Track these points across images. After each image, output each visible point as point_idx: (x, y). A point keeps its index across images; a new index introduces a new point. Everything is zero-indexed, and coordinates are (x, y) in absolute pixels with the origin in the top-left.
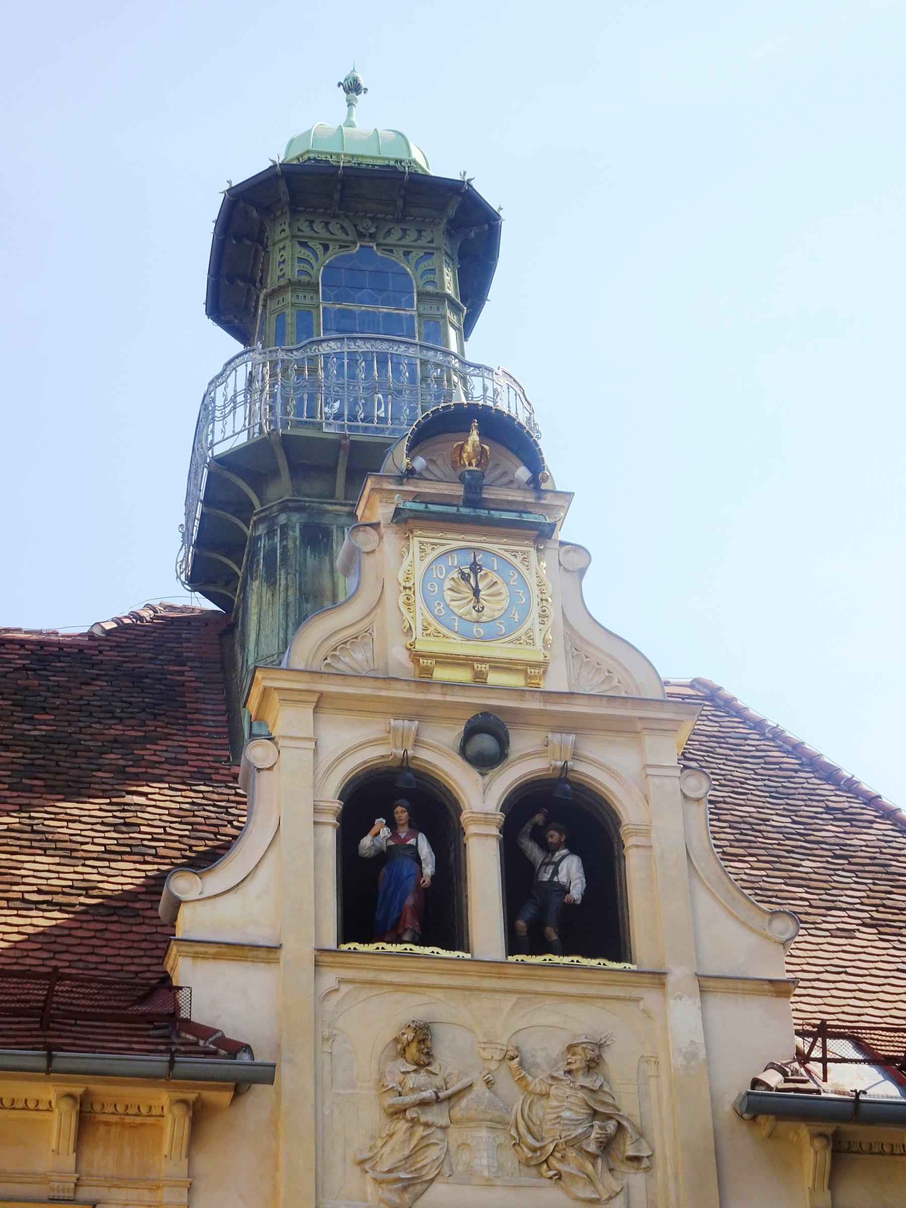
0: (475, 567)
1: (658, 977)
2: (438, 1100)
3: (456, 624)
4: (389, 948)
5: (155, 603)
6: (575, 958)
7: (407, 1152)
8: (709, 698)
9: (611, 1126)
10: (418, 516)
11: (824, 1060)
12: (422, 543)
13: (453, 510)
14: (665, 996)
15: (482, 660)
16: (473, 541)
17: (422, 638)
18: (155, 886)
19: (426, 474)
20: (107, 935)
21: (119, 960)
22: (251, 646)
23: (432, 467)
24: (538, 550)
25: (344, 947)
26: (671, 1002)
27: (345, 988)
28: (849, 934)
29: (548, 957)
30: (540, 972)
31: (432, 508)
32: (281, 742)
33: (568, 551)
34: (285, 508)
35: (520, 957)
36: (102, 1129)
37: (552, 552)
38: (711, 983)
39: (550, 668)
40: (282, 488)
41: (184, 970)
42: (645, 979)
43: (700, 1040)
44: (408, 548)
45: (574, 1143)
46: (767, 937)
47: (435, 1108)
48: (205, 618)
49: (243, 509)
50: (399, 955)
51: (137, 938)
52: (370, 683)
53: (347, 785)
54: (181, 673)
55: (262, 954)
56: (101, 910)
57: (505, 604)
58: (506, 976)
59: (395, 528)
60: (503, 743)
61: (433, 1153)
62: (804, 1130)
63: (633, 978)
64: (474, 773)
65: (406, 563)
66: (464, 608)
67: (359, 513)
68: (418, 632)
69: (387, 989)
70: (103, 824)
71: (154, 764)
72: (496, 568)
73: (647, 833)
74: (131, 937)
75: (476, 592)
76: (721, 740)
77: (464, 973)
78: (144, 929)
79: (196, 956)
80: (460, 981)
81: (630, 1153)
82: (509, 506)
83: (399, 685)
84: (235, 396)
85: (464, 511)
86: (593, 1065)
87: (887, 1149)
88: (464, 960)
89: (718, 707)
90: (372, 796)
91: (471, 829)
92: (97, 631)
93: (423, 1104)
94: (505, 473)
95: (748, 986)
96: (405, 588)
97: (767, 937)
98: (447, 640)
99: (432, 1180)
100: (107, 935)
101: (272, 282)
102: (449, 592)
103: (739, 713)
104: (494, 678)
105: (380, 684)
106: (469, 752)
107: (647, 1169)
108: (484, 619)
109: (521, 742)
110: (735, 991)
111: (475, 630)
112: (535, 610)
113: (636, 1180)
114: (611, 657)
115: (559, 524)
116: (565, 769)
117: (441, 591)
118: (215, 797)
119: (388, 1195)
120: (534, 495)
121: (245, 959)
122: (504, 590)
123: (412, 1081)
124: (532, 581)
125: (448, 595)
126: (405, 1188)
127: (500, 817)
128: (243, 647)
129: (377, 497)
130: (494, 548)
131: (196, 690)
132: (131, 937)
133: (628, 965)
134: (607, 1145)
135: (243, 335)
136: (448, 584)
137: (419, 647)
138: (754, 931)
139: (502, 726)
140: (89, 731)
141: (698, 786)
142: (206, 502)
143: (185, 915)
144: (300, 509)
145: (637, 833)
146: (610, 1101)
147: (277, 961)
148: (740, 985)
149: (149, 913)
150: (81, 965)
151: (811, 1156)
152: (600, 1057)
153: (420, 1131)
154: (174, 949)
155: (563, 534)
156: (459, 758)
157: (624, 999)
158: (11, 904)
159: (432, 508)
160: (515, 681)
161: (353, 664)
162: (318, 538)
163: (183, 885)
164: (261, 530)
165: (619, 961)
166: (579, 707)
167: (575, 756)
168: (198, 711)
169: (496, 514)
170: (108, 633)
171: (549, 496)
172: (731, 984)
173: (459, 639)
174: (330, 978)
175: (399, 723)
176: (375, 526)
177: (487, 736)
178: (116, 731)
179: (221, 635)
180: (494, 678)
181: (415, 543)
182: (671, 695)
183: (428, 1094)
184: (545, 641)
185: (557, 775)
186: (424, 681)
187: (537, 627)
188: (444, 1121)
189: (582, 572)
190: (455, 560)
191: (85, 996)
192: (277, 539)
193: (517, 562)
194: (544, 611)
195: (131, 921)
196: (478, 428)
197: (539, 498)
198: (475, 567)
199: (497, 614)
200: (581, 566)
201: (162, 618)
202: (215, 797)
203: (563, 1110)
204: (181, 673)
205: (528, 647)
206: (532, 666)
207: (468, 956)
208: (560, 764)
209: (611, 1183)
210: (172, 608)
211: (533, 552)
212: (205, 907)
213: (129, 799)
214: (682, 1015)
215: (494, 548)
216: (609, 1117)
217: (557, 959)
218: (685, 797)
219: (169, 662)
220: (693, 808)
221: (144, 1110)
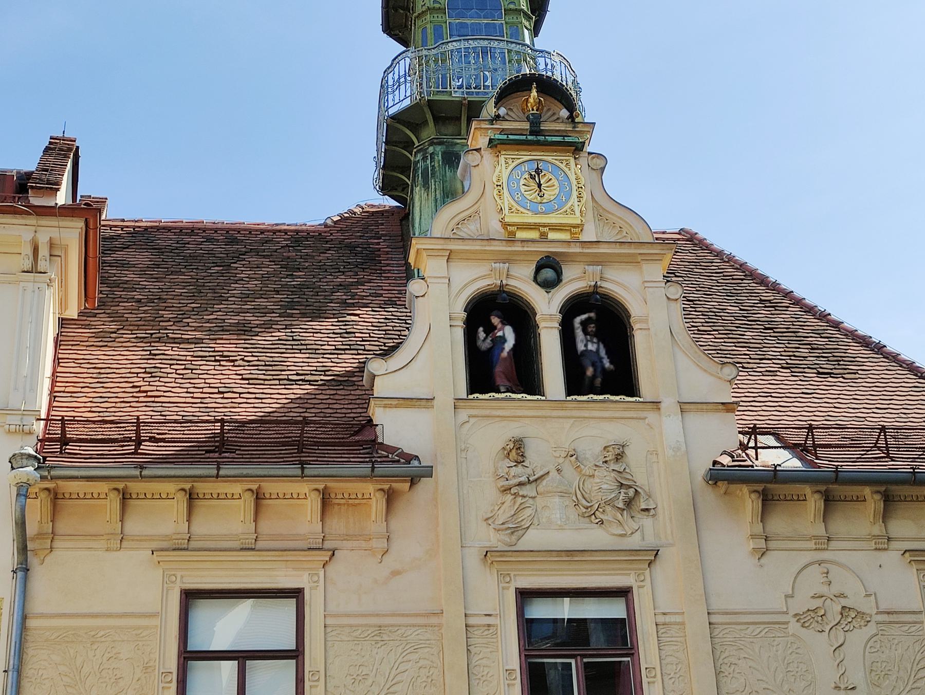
0: (538, 171)
1: (656, 404)
2: (529, 482)
4: (497, 395)
5: (363, 204)
6: (606, 396)
7: (513, 513)
8: (692, 239)
9: (631, 492)
10: (503, 142)
11: (756, 448)
13: (524, 137)
14: (660, 415)
16: (537, 155)
18: (361, 369)
19: (507, 117)
20: (337, 397)
21: (343, 411)
22: (417, 225)
23: (510, 113)
24: (575, 158)
25: (471, 397)
26: (664, 418)
27: (472, 420)
28: (773, 373)
29: (591, 396)
30: (585, 405)
31: (511, 137)
32: (428, 280)
33: (593, 158)
34: (432, 143)
35: (574, 397)
36: (336, 507)
37: (583, 159)
38: (687, 406)
39: (585, 227)
40: (429, 132)
41: (379, 414)
42: (649, 406)
43: (682, 439)
45: (608, 503)
46: (720, 378)
47: (528, 487)
48: (392, 211)
49: (408, 145)
50: (502, 399)
51: (354, 398)
52: (479, 242)
53: (468, 303)
54: (378, 244)
55: (423, 403)
56: (333, 383)
57: (557, 191)
58: (566, 409)
59: (490, 150)
60: (559, 273)
61: (528, 512)
62: (745, 489)
63: (641, 406)
64: (542, 291)
65: (497, 170)
66: (533, 196)
67: (469, 143)
68: (506, 211)
69: (498, 419)
70: (334, 333)
71: (362, 298)
73: (646, 321)
74: (351, 397)
75: (539, 185)
76: (696, 263)
77: (541, 408)
78: (358, 392)
79: (385, 406)
80: (539, 413)
81: (643, 507)
82: (557, 133)
83: (496, 243)
84: (399, 78)
85: (530, 138)
86: (619, 457)
87: (795, 498)
88: (541, 400)
89: (695, 245)
90: (490, 310)
91: (542, 324)
92: (329, 222)
93: (521, 484)
94: (554, 114)
95: (710, 407)
97: (720, 378)
99: (528, 528)
100: (337, 397)
101: (419, 10)
103: (708, 248)
104: (552, 236)
105: (485, 243)
106: (539, 280)
107: (653, 516)
108: (545, 201)
109: (569, 272)
110: (702, 410)
112: (575, 194)
113: (647, 522)
114: (620, 218)
115: (587, 142)
116: (596, 286)
118: (399, 314)
119: (503, 537)
120: (572, 125)
121: (414, 406)
122: (556, 183)
123: (513, 471)
124: (572, 177)
125: (523, 188)
126: (512, 533)
127: (559, 317)
128: (413, 226)
129: (478, 133)
130: (549, 158)
131: (387, 253)
132: (351, 397)
133: (638, 399)
134: (629, 503)
135: (405, 42)
136: (522, 182)
138: (712, 375)
139: (558, 263)
140: (325, 280)
141: (675, 291)
142: (387, 143)
143: (377, 381)
144: (440, 144)
145: (640, 322)
146: (630, 477)
147: (433, 407)
148: (704, 406)
149: (360, 383)
150: (322, 415)
151: (749, 502)
152: (623, 452)
153: (519, 500)
154: (372, 402)
155: (588, 149)
156: (534, 284)
157: (636, 418)
158: (281, 382)
159: (511, 137)
160: (565, 236)
161: (469, 233)
162: (452, 159)
163: (376, 366)
164: (419, 157)
165: (632, 396)
166: (603, 249)
167: (602, 279)
168: (388, 265)
169: (549, 139)
170: (335, 222)
171: (580, 125)
172: (700, 406)
173: (530, 214)
174: (463, 415)
175: (498, 265)
176: (478, 150)
177: (549, 270)
178: (341, 279)
179: (401, 220)
180: (552, 236)
181: (502, 159)
182: (657, 239)
183: (523, 479)
185: (591, 290)
186: (511, 239)
187: (576, 203)
188: (534, 494)
189: (602, 170)
190: (525, 167)
191: (324, 433)
192: (429, 162)
193: (563, 166)
195: (351, 388)
196: (536, 88)
197: (574, 127)
198: (538, 171)
199: (552, 198)
200: (602, 166)
201: (367, 212)
202: (399, 314)
203: (603, 484)
204: (378, 244)
206: (574, 227)
207: (543, 398)
208: (593, 283)
209: (632, 525)
210: (373, 206)
212: (388, 378)
213: (348, 318)
214: (670, 424)
215: (549, 158)
216: (630, 487)
217: (595, 397)
218: (668, 298)
219: (371, 238)
220: (673, 304)
221: (360, 496)
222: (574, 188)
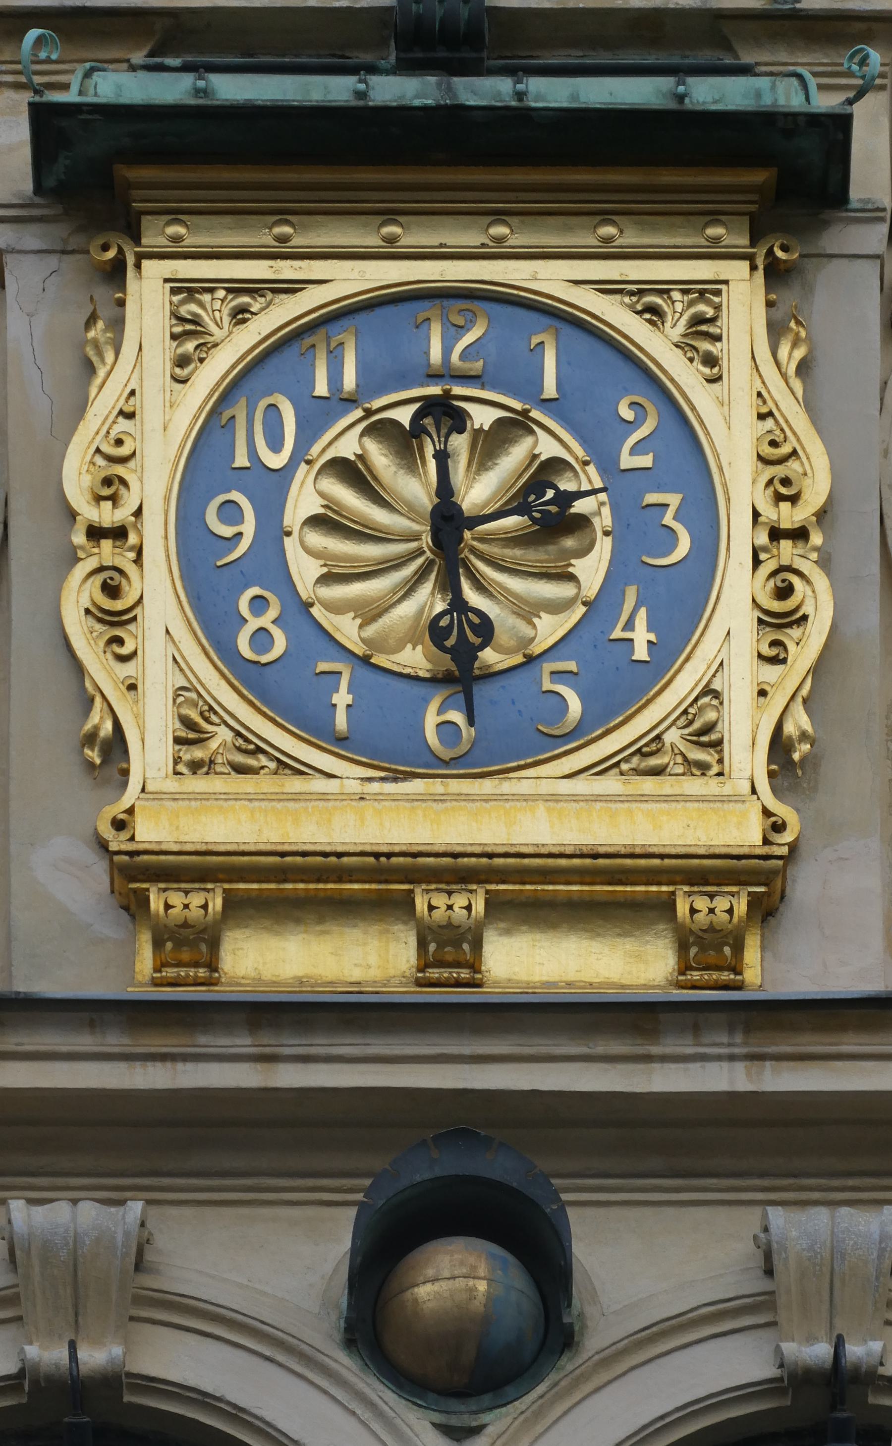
3: (342, 698)
12: (186, 289)
17: (172, 785)
24: (776, 275)
44: (117, 325)
68: (151, 753)
72: (550, 389)
96: (95, 533)
98: (295, 784)
102: (317, 539)
111: (431, 720)
117: (272, 531)
137: (149, 831)
173: (350, 774)
181: (148, 293)
193: (659, 346)
194: (784, 592)
211: (744, 298)
215: (550, 279)
222: (739, 537)
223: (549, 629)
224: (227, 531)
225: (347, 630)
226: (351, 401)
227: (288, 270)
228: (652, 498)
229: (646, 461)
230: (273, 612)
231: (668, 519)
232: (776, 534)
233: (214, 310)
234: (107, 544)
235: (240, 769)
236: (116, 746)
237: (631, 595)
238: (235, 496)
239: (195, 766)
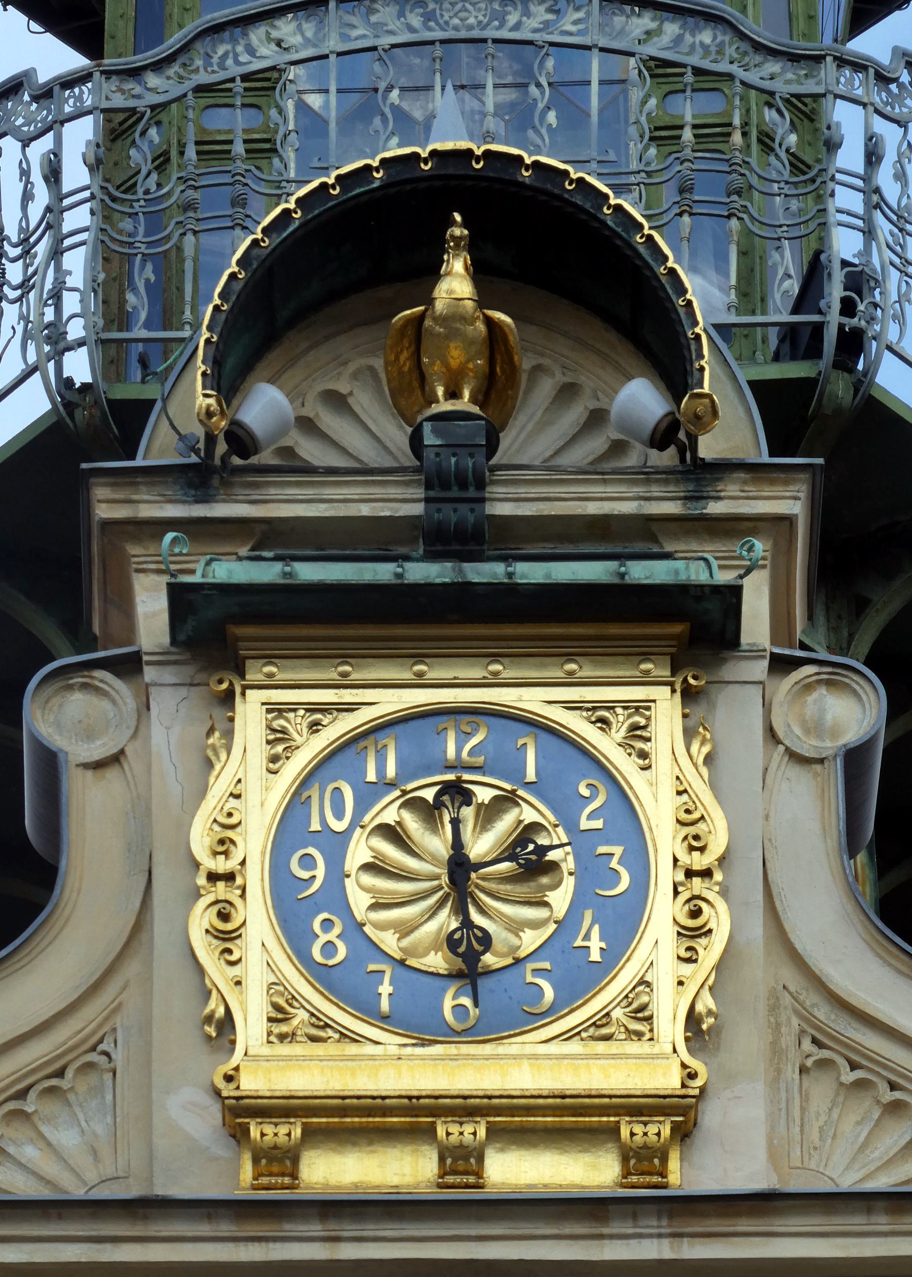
3: (385, 989)
12: (277, 710)
15: (465, 1108)
17: (266, 1050)
24: (689, 695)
44: (229, 734)
68: (251, 1029)
72: (531, 776)
96: (213, 877)
102: (368, 879)
111: (448, 1003)
117: (337, 874)
137: (252, 1082)
173: (391, 1042)
184: (693, 1019)
193: (607, 745)
194: (695, 913)
205: (633, 1047)
211: (667, 711)
215: (530, 700)
223: (530, 940)
224: (305, 875)
225: (389, 942)
226: (392, 785)
227: (348, 696)
228: (602, 849)
229: (598, 824)
230: (337, 930)
231: (614, 864)
232: (690, 874)
233: (297, 724)
234: (221, 885)
235: (314, 1039)
236: (227, 1024)
237: (588, 916)
238: (311, 850)
239: (282, 1037)
